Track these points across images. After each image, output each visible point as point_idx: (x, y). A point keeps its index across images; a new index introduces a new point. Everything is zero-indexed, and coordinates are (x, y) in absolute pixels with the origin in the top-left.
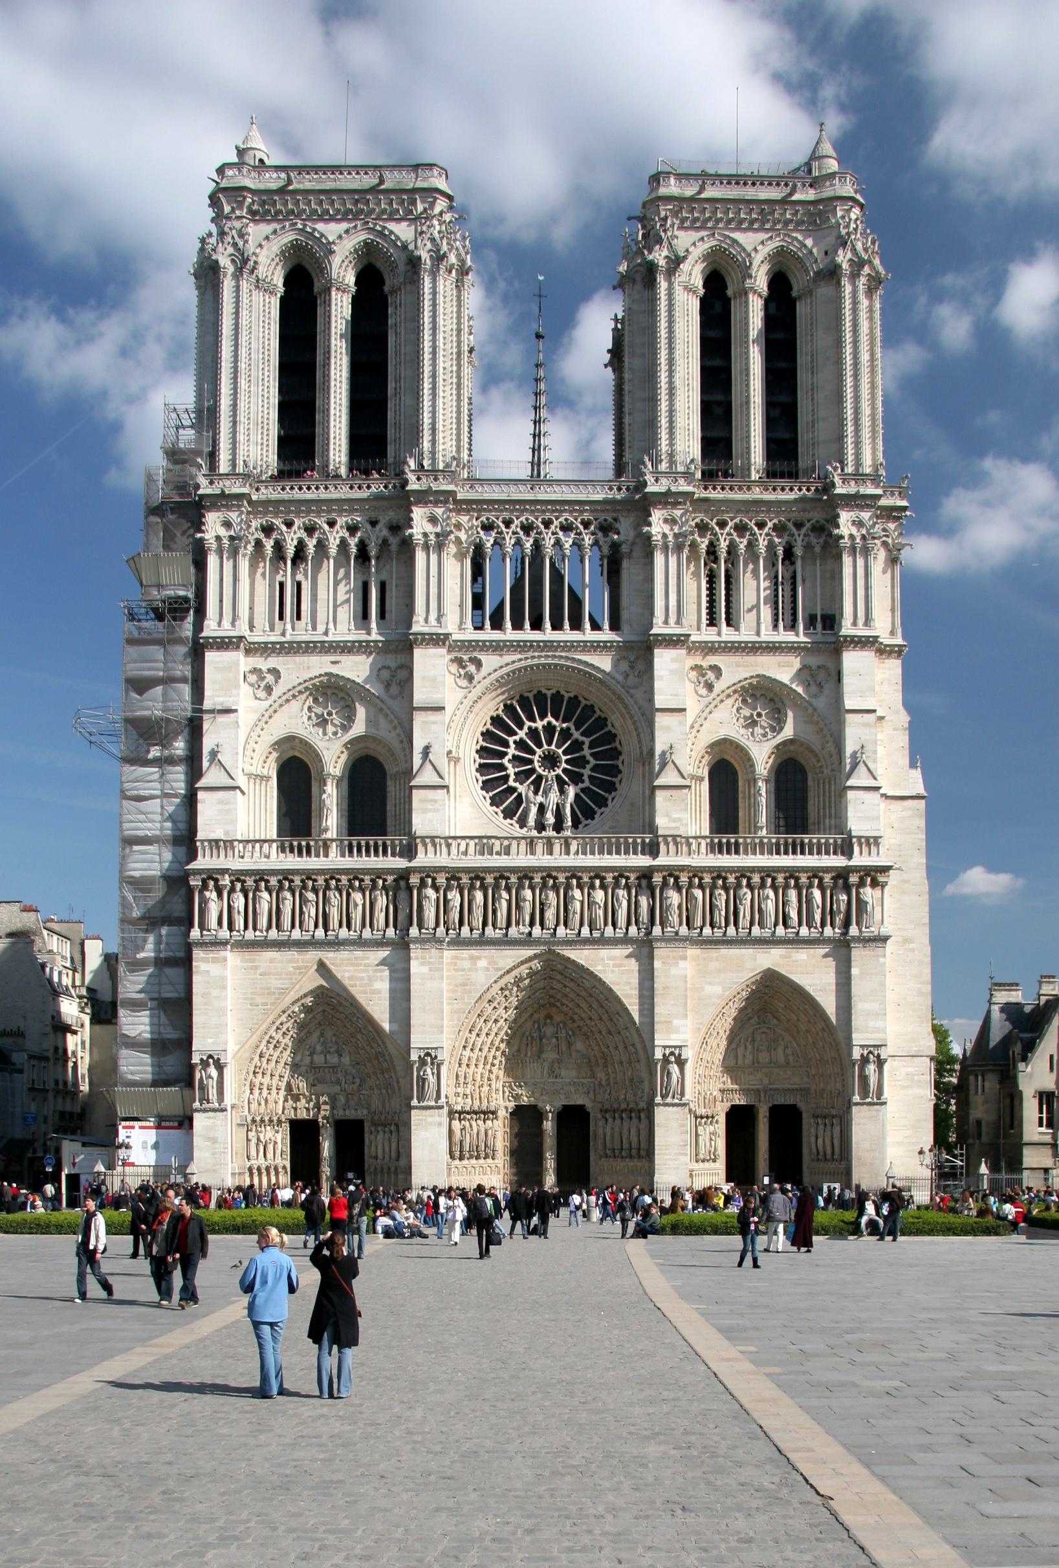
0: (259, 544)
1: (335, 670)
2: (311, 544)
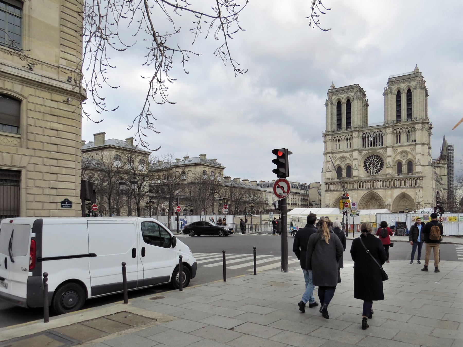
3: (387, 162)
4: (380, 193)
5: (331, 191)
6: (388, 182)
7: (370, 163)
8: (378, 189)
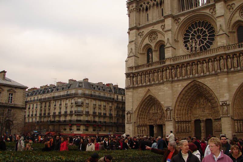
0: (140, 9)
1: (153, 29)
2: (148, 6)
3: (218, 26)
4: (209, 82)
5: (134, 88)
6: (222, 61)
7: (192, 35)
8: (204, 77)
